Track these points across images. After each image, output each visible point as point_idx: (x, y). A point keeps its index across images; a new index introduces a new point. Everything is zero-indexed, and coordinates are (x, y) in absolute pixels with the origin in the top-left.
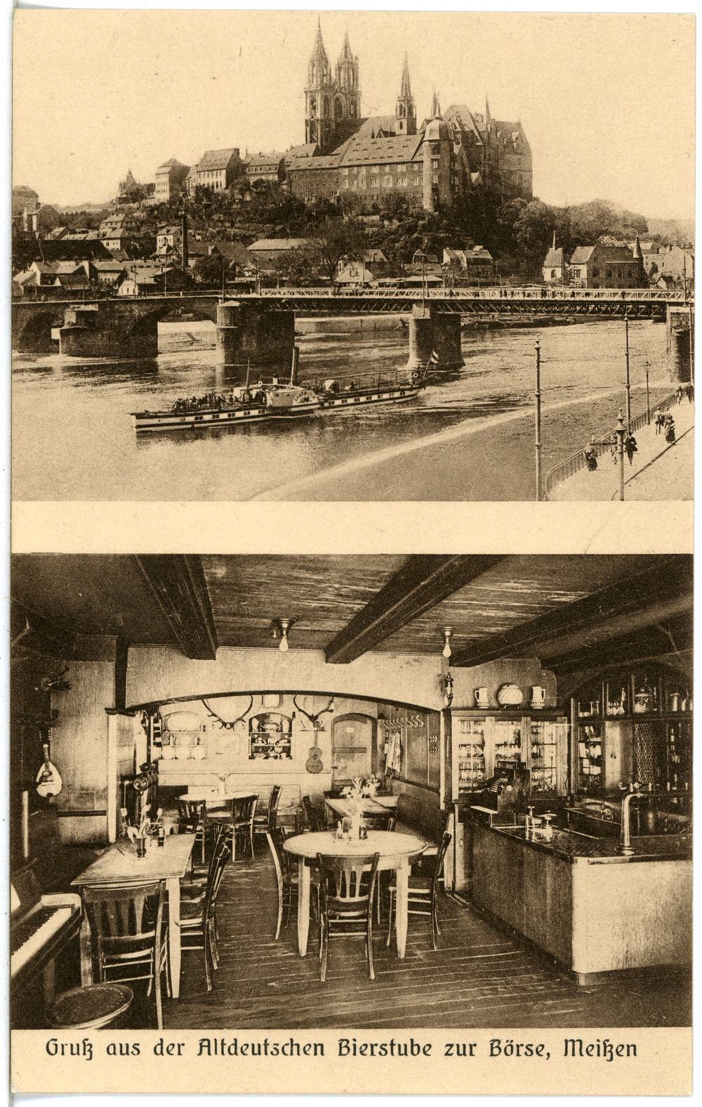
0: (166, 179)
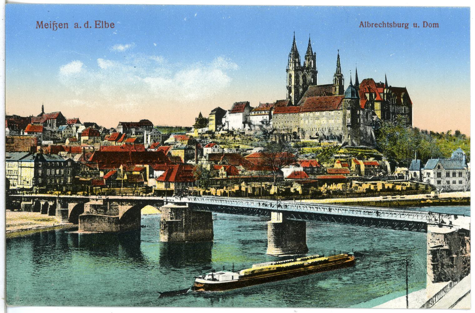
0: (213, 117)
